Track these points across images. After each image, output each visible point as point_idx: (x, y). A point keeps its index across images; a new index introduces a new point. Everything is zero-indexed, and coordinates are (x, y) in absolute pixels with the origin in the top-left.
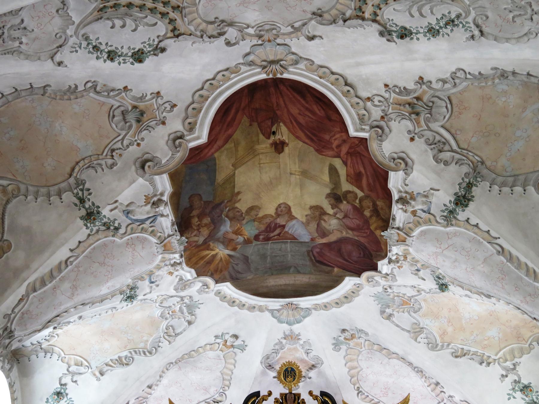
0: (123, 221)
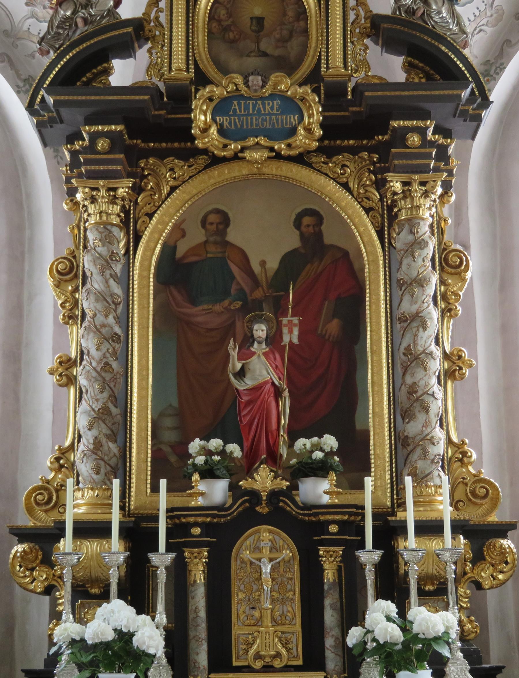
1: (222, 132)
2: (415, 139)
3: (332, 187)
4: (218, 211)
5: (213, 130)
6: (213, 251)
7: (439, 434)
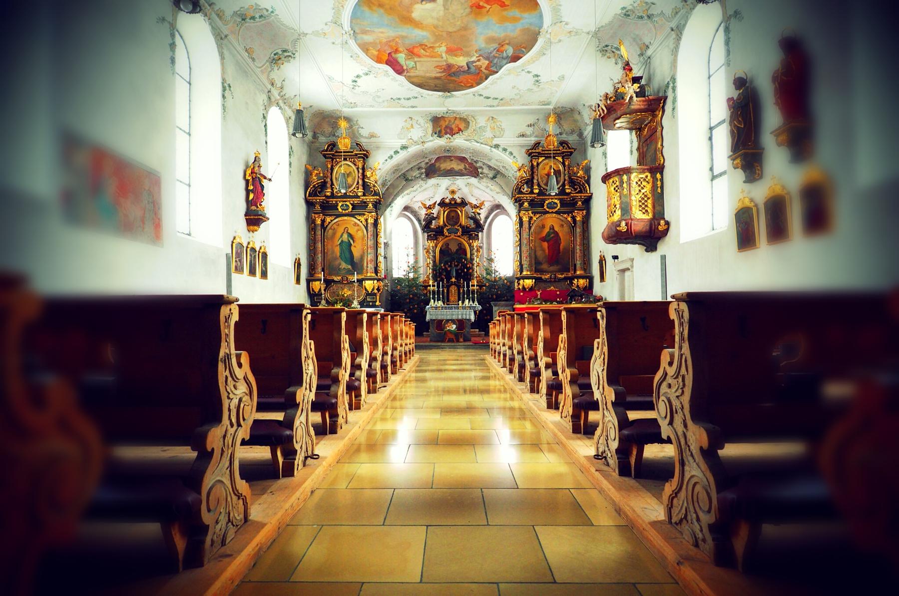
0: (413, 178)
2: (474, 235)
3: (463, 240)
6: (447, 249)
7: (476, 274)
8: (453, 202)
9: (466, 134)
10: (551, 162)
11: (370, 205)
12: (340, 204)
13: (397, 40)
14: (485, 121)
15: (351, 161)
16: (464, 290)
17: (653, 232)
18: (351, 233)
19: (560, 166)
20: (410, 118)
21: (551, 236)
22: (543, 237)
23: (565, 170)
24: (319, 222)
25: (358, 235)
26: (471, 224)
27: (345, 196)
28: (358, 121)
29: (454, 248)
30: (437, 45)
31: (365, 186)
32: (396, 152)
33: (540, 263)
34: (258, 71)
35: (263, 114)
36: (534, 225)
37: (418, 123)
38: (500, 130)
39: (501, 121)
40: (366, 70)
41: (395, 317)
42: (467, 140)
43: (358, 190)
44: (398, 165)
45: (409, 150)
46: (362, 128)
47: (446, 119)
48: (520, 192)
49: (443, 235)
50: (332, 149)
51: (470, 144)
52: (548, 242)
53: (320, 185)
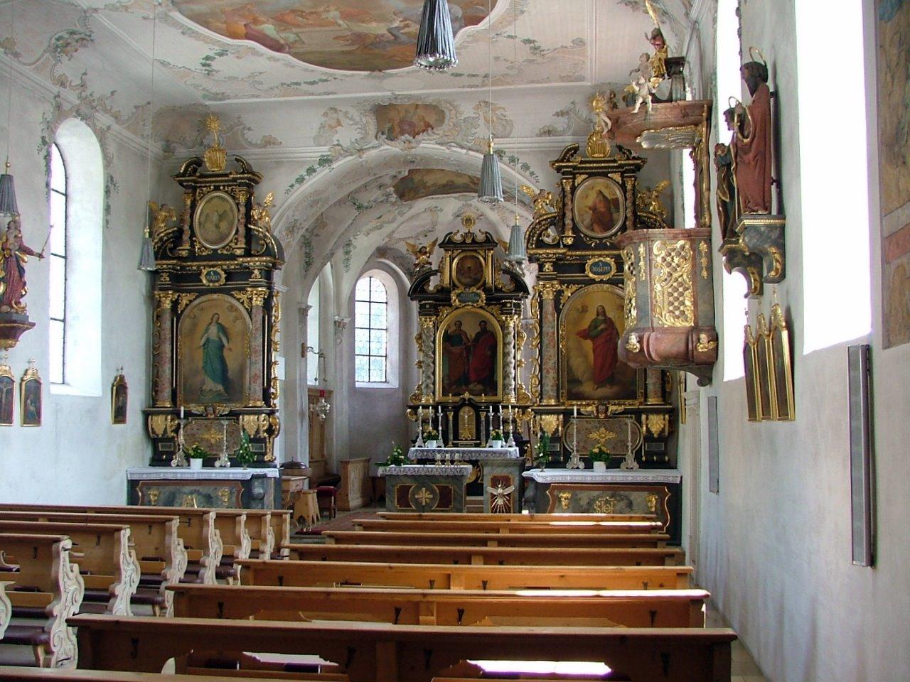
1: (459, 301)
3: (489, 315)
4: (459, 321)
5: (457, 301)
6: (458, 332)
8: (469, 241)
9: (441, 132)
10: (599, 183)
11: (256, 272)
12: (205, 272)
13: (249, 6)
14: (474, 108)
15: (227, 192)
16: (487, 417)
17: (690, 353)
18: (223, 323)
19: (618, 192)
20: (332, 109)
21: (599, 328)
22: (585, 330)
23: (626, 199)
24: (167, 305)
25: (235, 329)
26: (504, 282)
27: (214, 256)
28: (239, 118)
29: (471, 330)
30: (322, 9)
31: (249, 235)
32: (311, 171)
33: (579, 382)
34: (26, 69)
35: (43, 138)
36: (567, 306)
37: (349, 115)
38: (505, 123)
39: (504, 109)
40: (217, 49)
41: (167, 523)
42: (441, 144)
43: (236, 244)
44: (317, 192)
45: (335, 165)
46: (249, 129)
47: (399, 108)
48: (541, 244)
49: (450, 305)
50: (195, 170)
51: (448, 151)
52: (593, 339)
53: (172, 238)
